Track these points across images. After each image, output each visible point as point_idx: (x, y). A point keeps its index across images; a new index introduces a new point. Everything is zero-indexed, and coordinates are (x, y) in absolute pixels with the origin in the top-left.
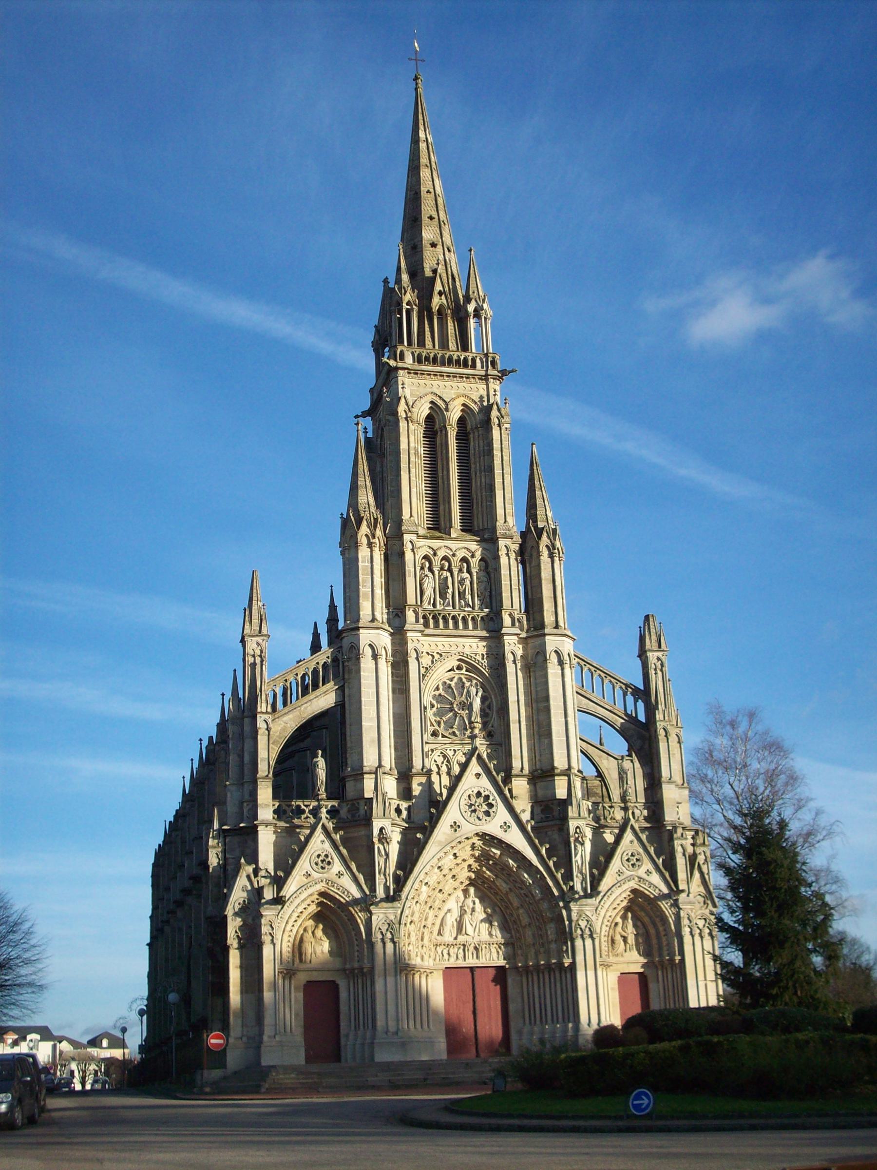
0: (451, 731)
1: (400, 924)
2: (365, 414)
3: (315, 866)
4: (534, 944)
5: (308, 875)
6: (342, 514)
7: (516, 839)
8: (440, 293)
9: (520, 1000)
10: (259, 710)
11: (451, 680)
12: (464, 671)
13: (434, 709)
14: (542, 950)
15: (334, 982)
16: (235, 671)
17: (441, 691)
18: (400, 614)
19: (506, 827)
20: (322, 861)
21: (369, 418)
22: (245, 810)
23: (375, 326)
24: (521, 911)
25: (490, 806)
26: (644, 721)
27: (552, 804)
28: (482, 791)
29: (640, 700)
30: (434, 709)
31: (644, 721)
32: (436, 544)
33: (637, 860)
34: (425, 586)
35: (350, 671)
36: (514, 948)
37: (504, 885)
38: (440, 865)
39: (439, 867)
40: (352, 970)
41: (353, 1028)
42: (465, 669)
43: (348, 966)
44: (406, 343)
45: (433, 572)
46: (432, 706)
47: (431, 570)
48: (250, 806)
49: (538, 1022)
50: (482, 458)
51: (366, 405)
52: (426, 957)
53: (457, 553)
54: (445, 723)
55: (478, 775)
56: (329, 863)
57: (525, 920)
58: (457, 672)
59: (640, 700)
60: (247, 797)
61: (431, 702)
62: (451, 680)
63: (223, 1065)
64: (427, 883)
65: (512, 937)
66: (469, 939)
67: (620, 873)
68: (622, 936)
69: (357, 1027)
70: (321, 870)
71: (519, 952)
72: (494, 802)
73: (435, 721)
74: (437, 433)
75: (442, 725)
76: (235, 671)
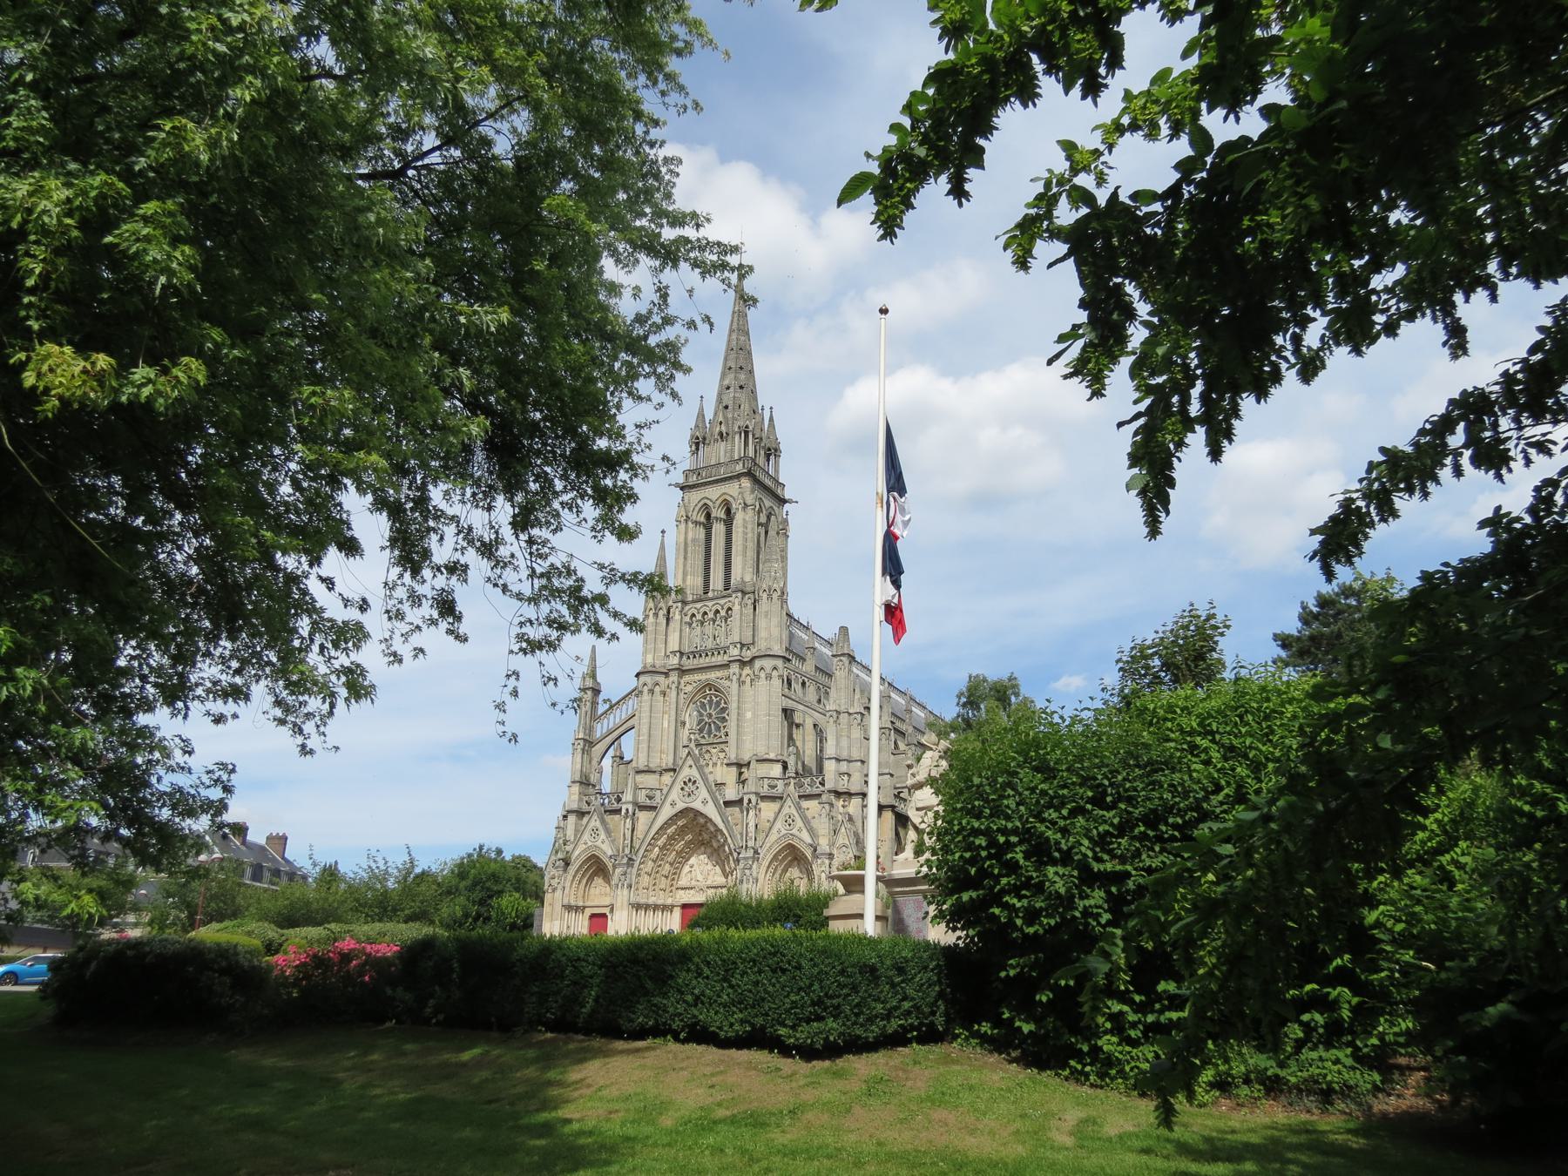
19: (705, 802)
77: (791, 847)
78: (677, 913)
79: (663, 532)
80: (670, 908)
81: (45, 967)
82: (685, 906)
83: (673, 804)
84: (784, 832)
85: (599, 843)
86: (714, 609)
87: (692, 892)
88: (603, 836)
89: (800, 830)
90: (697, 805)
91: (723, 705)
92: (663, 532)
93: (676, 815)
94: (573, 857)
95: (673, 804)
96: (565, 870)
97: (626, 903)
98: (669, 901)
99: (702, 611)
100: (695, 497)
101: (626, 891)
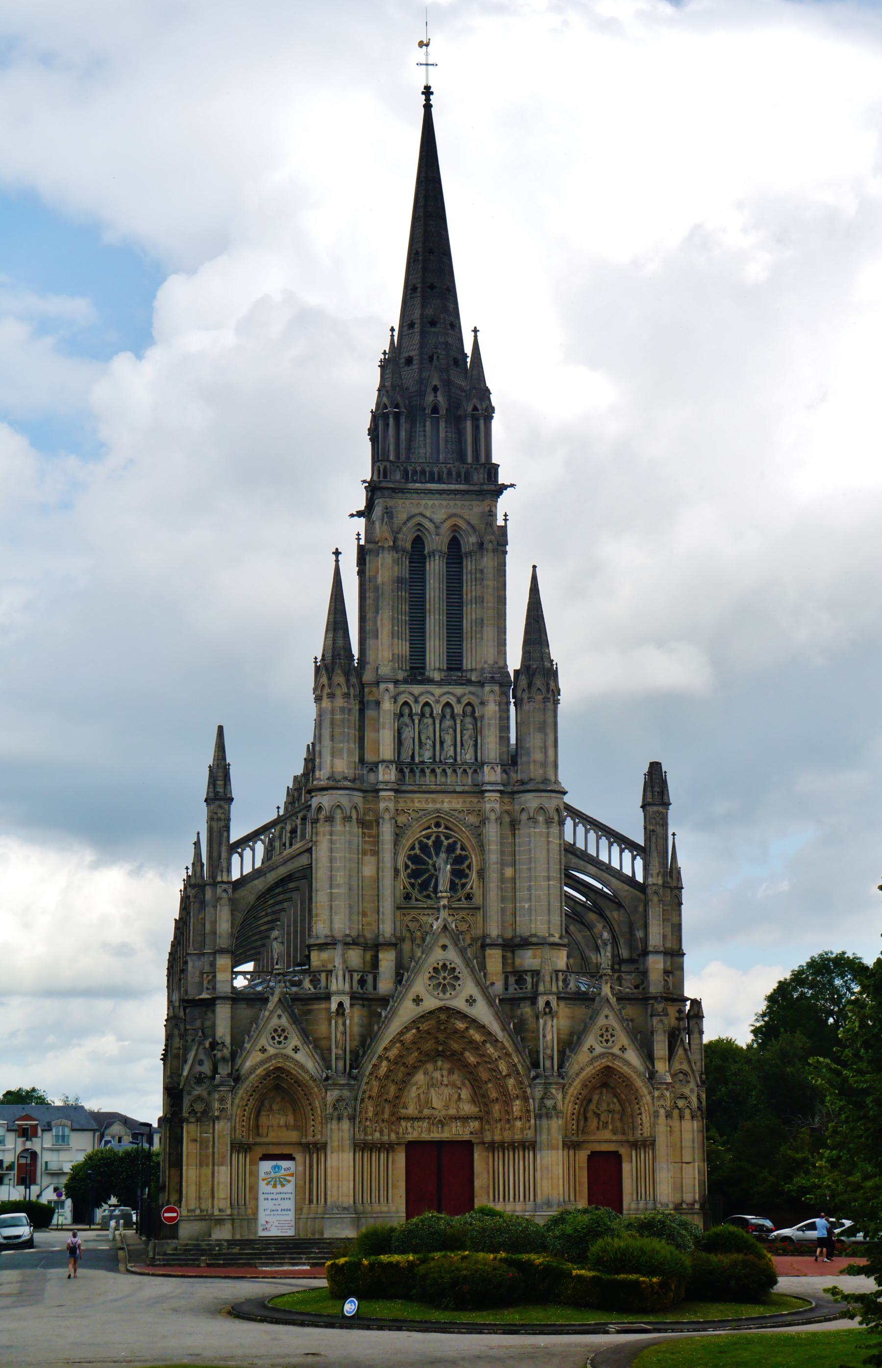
0: (425, 893)
1: (356, 1100)
2: (360, 514)
3: (271, 1042)
4: (500, 1120)
5: (263, 1050)
6: (316, 658)
7: (482, 1012)
8: (435, 389)
9: (485, 1175)
10: (219, 879)
11: (428, 838)
12: (440, 830)
13: (409, 871)
14: (507, 1126)
15: (291, 1155)
16: (198, 833)
17: (417, 851)
18: (374, 769)
19: (471, 1001)
20: (279, 1036)
21: (363, 520)
22: (205, 982)
23: (372, 412)
24: (490, 1085)
25: (457, 978)
26: (642, 881)
27: (526, 975)
28: (448, 964)
29: (638, 857)
30: (409, 871)
31: (642, 881)
32: (417, 689)
33: (612, 1036)
34: (404, 736)
35: (317, 834)
36: (482, 1123)
37: (472, 1059)
38: (402, 1038)
39: (402, 1041)
40: (308, 1144)
41: (307, 1202)
42: (443, 826)
43: (304, 1141)
44: (392, 458)
45: (413, 721)
46: (407, 867)
47: (411, 715)
48: (210, 977)
49: (501, 1199)
50: (474, 587)
51: (362, 506)
52: (386, 1131)
53: (441, 700)
54: (420, 885)
55: (444, 947)
56: (286, 1038)
57: (494, 1095)
58: (435, 830)
59: (638, 857)
60: (207, 968)
61: (406, 863)
62: (428, 838)
63: (175, 1236)
64: (387, 1057)
65: (480, 1111)
66: (436, 1113)
67: (591, 1049)
68: (595, 1113)
69: (311, 1201)
70: (277, 1045)
71: (487, 1127)
72: (460, 975)
73: (410, 883)
74: (425, 558)
75: (417, 887)
76: (198, 833)
77: (608, 1071)
78: (400, 1159)
79: (337, 553)
80: (389, 1148)
81: (785, 1284)
82: (414, 1148)
83: (418, 1000)
84: (599, 1050)
85: (289, 1051)
86: (444, 700)
87: (425, 1124)
88: (295, 1040)
89: (623, 1049)
90: (459, 1003)
91: (458, 852)
92: (337, 553)
93: (422, 1017)
94: (243, 1072)
95: (418, 1000)
96: (233, 1090)
97: (347, 1143)
98: (393, 1136)
99: (423, 700)
100: (404, 507)
101: (346, 1125)
